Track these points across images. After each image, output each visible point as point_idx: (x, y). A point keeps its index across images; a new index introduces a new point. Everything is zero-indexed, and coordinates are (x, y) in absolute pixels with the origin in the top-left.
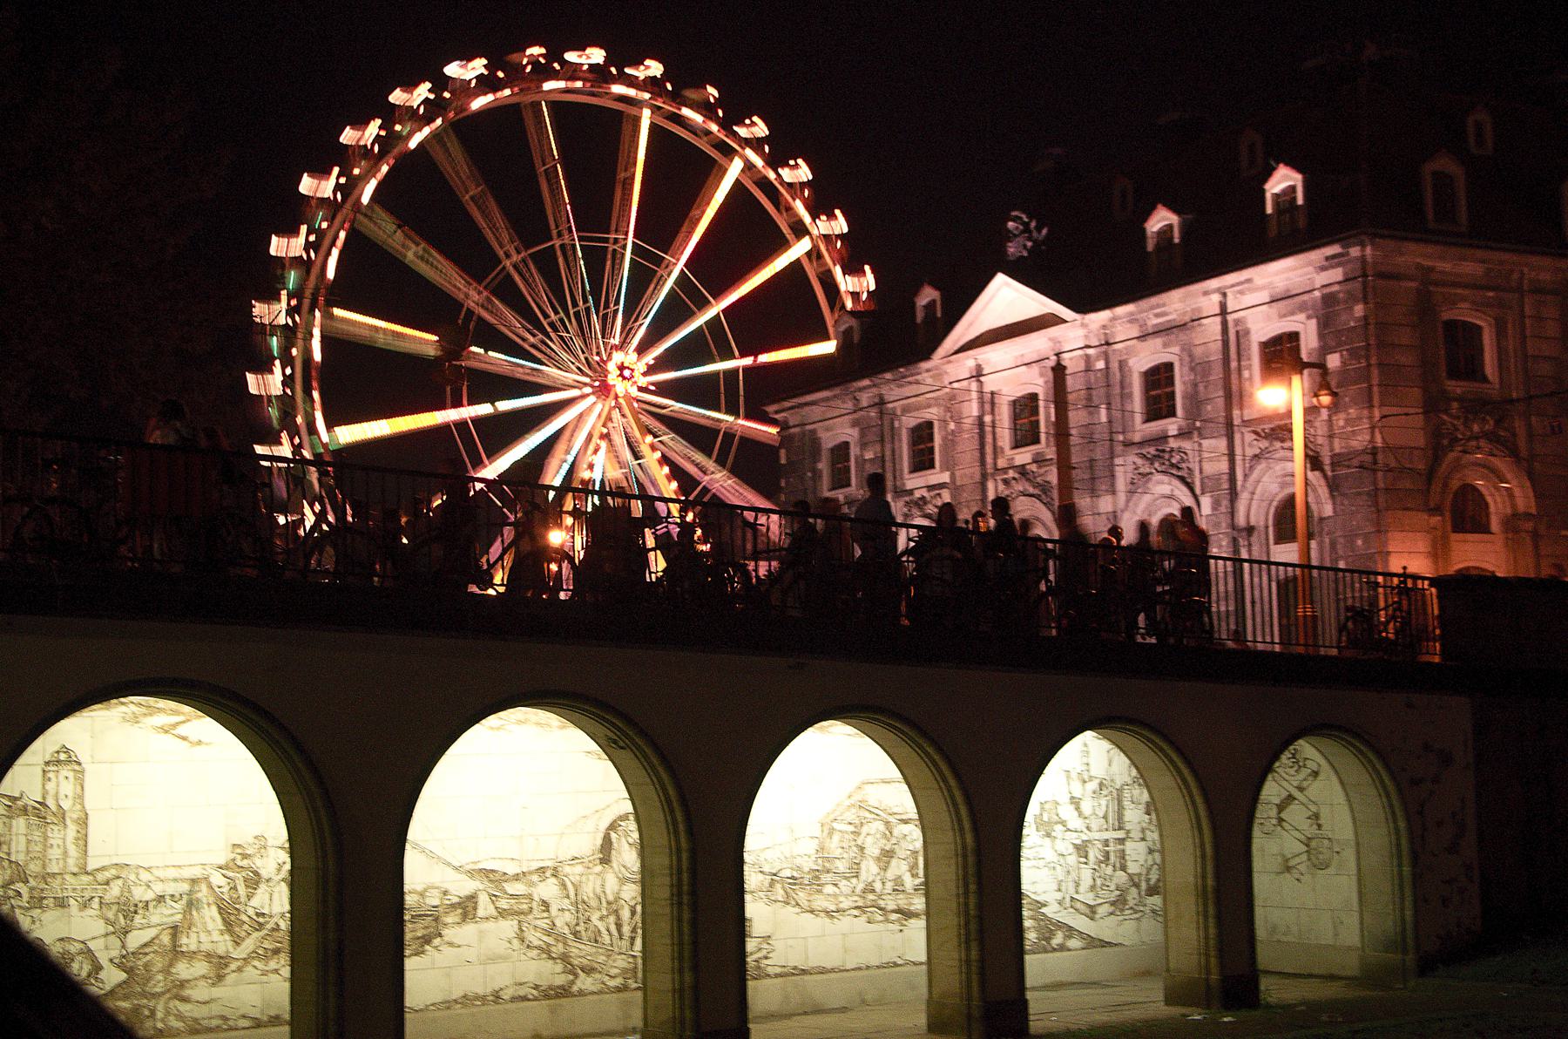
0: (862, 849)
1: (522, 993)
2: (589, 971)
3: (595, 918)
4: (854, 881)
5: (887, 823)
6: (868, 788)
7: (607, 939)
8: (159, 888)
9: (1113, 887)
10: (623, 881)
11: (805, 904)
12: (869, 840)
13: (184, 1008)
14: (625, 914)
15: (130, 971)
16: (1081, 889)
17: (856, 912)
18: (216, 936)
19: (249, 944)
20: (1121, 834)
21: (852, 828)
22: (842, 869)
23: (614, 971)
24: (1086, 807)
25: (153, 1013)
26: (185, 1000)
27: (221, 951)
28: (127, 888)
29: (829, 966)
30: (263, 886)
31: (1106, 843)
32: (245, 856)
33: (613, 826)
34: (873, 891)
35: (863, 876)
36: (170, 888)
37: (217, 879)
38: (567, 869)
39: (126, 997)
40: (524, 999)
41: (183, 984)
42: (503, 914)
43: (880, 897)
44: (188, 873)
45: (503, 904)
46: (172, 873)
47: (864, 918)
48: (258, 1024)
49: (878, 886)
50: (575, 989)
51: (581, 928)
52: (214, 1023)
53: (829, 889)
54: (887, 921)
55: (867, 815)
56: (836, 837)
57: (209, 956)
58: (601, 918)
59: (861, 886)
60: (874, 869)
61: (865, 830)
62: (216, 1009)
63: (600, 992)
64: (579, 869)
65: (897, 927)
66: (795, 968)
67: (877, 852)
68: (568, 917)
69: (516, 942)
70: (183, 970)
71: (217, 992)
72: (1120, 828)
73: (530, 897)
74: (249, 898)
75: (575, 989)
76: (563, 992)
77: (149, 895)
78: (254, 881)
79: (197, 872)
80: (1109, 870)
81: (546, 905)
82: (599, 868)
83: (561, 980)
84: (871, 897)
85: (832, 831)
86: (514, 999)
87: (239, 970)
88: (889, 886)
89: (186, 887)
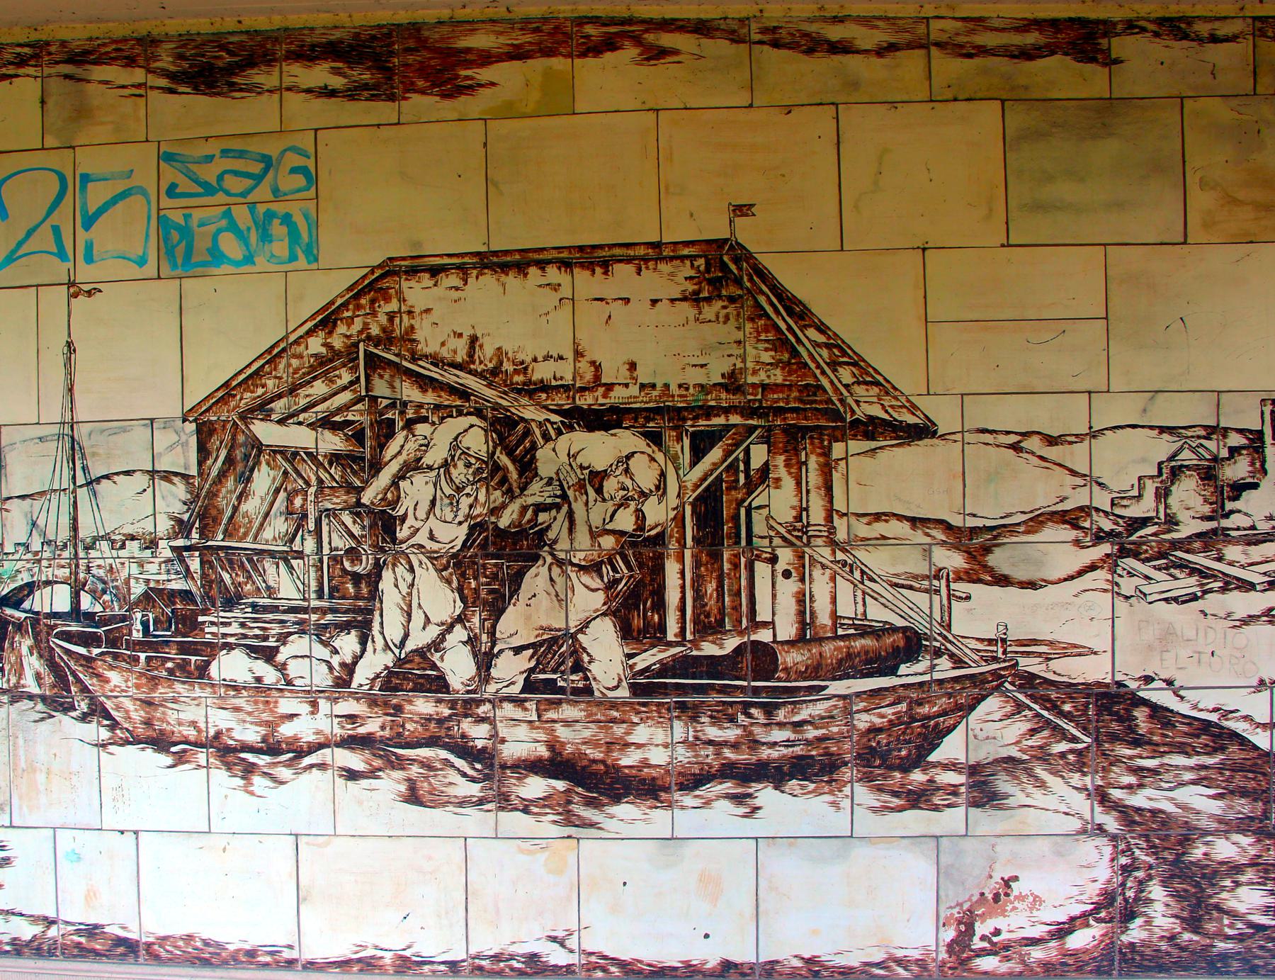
0: (384, 523)
4: (348, 643)
5: (503, 427)
6: (417, 292)
11: (131, 712)
12: (418, 490)
17: (355, 760)
21: (332, 442)
34: (438, 684)
35: (390, 622)
47: (391, 783)
49: (458, 665)
53: (233, 666)
54: (504, 802)
55: (410, 392)
56: (263, 479)
59: (374, 663)
60: (439, 600)
61: (398, 448)
65: (547, 826)
66: (93, 931)
67: (453, 535)
84: (423, 705)
88: (510, 670)
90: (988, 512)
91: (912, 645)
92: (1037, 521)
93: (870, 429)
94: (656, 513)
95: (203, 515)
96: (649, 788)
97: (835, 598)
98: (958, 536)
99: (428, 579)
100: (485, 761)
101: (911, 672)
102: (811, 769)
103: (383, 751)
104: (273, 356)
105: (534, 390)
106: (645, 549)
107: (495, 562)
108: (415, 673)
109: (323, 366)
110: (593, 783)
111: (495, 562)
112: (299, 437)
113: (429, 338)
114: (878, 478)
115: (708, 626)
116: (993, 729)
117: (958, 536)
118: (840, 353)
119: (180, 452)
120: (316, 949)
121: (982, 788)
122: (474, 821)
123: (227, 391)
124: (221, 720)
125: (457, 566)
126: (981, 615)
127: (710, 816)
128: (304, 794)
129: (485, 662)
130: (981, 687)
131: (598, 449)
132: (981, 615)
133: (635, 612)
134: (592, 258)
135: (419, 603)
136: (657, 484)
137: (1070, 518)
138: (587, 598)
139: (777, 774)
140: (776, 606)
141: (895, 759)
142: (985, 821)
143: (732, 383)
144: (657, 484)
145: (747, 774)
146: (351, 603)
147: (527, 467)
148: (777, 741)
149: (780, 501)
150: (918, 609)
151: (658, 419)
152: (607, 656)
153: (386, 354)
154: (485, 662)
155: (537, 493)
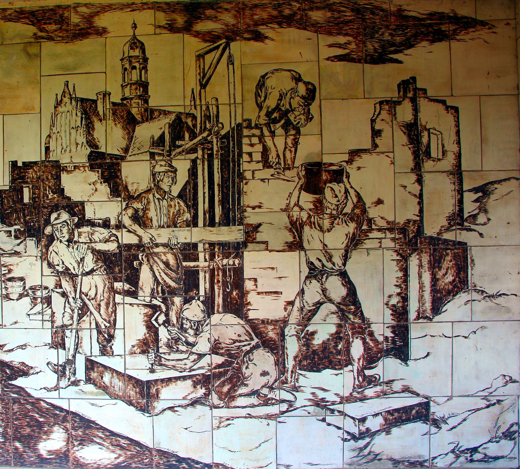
16: (117, 346)
20: (232, 234)
24: (136, 174)
31: (189, 251)
72: (227, 221)
80: (194, 311)
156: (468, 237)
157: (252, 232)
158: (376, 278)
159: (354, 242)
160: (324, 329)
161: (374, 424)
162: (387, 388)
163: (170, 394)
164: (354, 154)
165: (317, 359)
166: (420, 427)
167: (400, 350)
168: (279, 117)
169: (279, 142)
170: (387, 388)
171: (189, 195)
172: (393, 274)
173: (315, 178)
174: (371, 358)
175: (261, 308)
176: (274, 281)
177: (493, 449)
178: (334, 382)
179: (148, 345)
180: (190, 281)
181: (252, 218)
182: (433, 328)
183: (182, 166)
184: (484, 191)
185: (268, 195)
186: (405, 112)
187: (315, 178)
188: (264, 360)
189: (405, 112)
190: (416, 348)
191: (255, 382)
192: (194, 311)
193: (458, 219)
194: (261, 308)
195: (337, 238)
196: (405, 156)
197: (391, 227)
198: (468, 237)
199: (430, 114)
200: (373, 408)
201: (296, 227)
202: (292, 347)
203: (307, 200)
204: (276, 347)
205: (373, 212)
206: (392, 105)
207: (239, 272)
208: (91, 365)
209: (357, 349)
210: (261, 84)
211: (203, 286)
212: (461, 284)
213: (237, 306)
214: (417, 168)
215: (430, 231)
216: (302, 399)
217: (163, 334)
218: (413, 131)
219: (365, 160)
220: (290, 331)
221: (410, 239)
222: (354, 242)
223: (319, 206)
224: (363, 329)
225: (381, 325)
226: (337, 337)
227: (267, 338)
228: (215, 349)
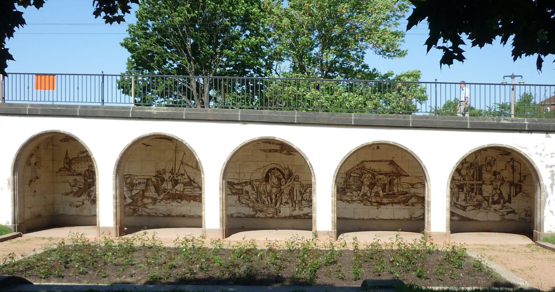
0: (362, 182)
1: (240, 215)
2: (261, 211)
3: (263, 197)
4: (359, 192)
5: (373, 174)
6: (366, 163)
7: (267, 203)
8: (139, 181)
9: (475, 200)
10: (272, 187)
12: (365, 180)
13: (146, 210)
14: (274, 197)
15: (133, 200)
16: (459, 200)
18: (153, 193)
19: (162, 196)
21: (358, 175)
22: (354, 188)
23: (269, 212)
25: (139, 210)
26: (146, 208)
27: (155, 197)
28: (131, 180)
29: (347, 217)
30: (165, 182)
31: (473, 185)
32: (160, 174)
33: (269, 171)
34: (367, 195)
35: (363, 190)
36: (142, 181)
37: (153, 179)
38: (254, 183)
39: (132, 206)
40: (240, 217)
41: (146, 204)
42: (234, 194)
43: (369, 197)
44: (146, 177)
45: (234, 191)
46: (143, 177)
47: (362, 204)
48: (165, 216)
49: (368, 194)
50: (256, 216)
51: (259, 199)
52: (154, 214)
53: (349, 194)
54: (372, 205)
56: (352, 178)
57: (152, 198)
58: (265, 197)
59: (361, 194)
60: (367, 189)
61: (364, 176)
62: (154, 211)
63: (265, 218)
64: (258, 183)
68: (254, 196)
69: (238, 202)
70: (145, 201)
71: (154, 207)
72: (479, 180)
73: (242, 190)
74: (162, 184)
75: (256, 216)
76: (253, 217)
77: (137, 182)
78: (163, 180)
79: (148, 177)
81: (247, 192)
82: (264, 183)
83: (252, 213)
85: (350, 176)
86: (237, 217)
87: (160, 202)
88: (373, 194)
89: (146, 181)
90: (413, 182)
91: (407, 193)
92: (417, 183)
93: (404, 175)
94: (385, 182)
95: (346, 181)
96: (385, 204)
97: (400, 189)
98: (411, 184)
99: (366, 187)
100: (371, 202)
101: (407, 195)
102: (398, 203)
103: (362, 201)
104: (353, 168)
105: (375, 172)
106: (385, 185)
107: (372, 186)
108: (365, 194)
109: (357, 169)
110: (380, 204)
111: (372, 186)
112: (355, 175)
113: (366, 167)
114: (404, 179)
115: (390, 191)
116: (414, 200)
117: (411, 184)
118: (401, 169)
119: (344, 176)
120: (356, 217)
121: (413, 205)
122: (371, 206)
123: (349, 171)
124: (347, 198)
125: (369, 186)
126: (413, 191)
127: (389, 207)
128: (355, 205)
129: (371, 194)
130: (412, 197)
131: (381, 176)
132: (413, 191)
133: (384, 190)
134: (381, 161)
135: (365, 189)
136: (386, 180)
137: (420, 183)
138: (380, 189)
139: (395, 203)
140: (395, 189)
141: (405, 202)
142: (413, 207)
143: (392, 172)
144: (386, 180)
145: (393, 203)
146: (359, 188)
147: (375, 178)
148: (395, 201)
149: (396, 181)
150: (407, 190)
151: (386, 174)
152: (381, 193)
153: (363, 168)
154: (371, 194)
155: (376, 180)
156: (522, 184)
157: (484, 182)
158: (505, 190)
159: (501, 184)
160: (496, 198)
161: (505, 213)
162: (507, 208)
163: (468, 208)
164: (502, 170)
165: (494, 203)
166: (513, 214)
167: (509, 201)
168: (489, 164)
169: (489, 168)
170: (507, 208)
171: (473, 176)
172: (508, 189)
173: (495, 174)
174: (504, 203)
175: (485, 194)
176: (487, 190)
177: (526, 218)
178: (498, 207)
179: (465, 200)
180: (472, 190)
181: (484, 180)
182: (515, 198)
183: (472, 171)
184: (525, 176)
185: (487, 176)
186: (511, 163)
187: (495, 174)
188: (486, 203)
189: (511, 163)
190: (512, 201)
191: (484, 206)
192: (473, 194)
193: (520, 181)
194: (485, 194)
195: (499, 183)
196: (511, 170)
197: (508, 182)
198: (522, 184)
199: (516, 164)
200: (504, 211)
201: (492, 181)
202: (490, 201)
203: (493, 177)
204: (488, 201)
205: (505, 179)
206: (509, 162)
207: (481, 188)
208: (454, 203)
209: (502, 201)
210: (486, 158)
211: (475, 191)
212: (520, 191)
213: (481, 194)
214: (513, 173)
215: (515, 182)
216: (492, 209)
217: (468, 198)
218: (513, 167)
219: (504, 171)
220: (490, 198)
221: (511, 184)
222: (501, 184)
223: (496, 178)
224: (503, 198)
225: (506, 198)
226: (498, 199)
227: (486, 199)
228: (477, 201)
